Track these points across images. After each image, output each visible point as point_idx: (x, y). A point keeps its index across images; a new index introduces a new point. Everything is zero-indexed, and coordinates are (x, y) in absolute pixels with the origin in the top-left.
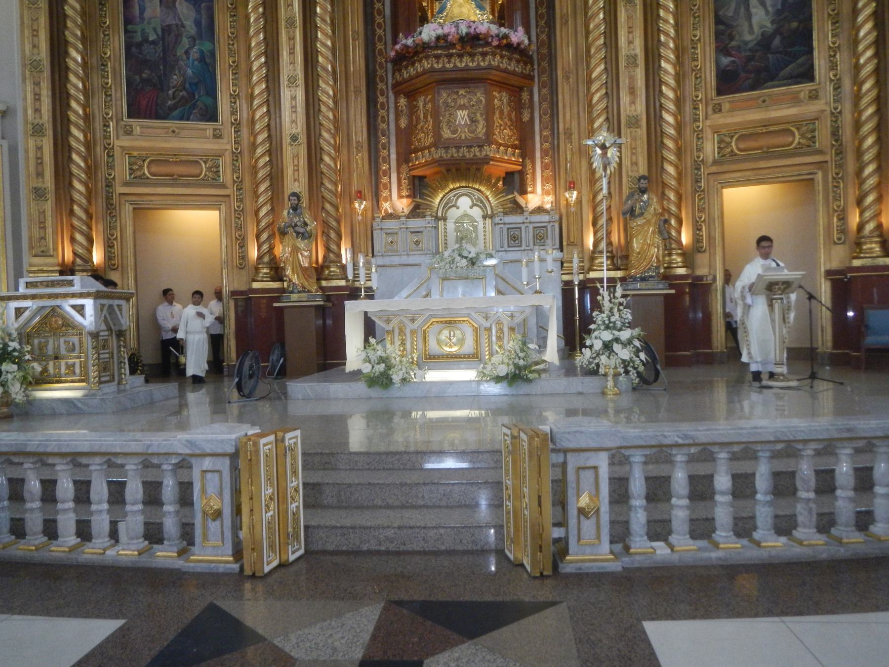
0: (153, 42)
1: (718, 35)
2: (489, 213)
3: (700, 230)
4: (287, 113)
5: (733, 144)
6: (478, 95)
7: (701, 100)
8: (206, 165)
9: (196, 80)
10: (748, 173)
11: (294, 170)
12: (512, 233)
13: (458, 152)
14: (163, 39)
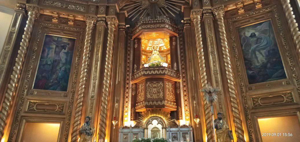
0: (49, 65)
1: (246, 64)
2: (165, 126)
3: (252, 136)
4: (91, 88)
5: (259, 101)
6: (161, 83)
8: (58, 106)
9: (61, 77)
10: (267, 113)
11: (91, 109)
12: (174, 135)
13: (153, 103)
14: (53, 64)
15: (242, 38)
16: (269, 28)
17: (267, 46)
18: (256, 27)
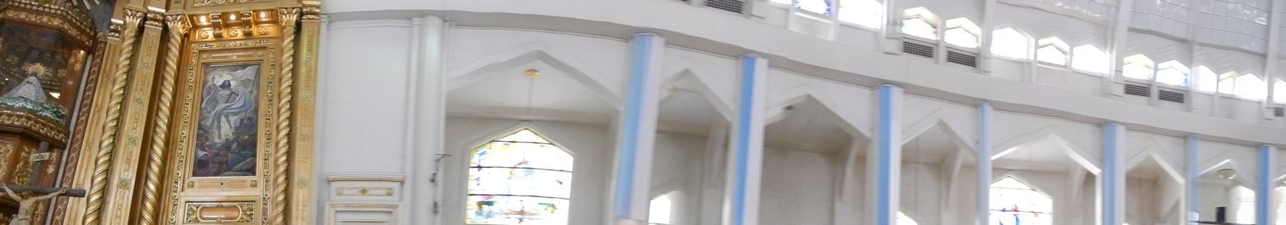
7: (180, 177)
15: (207, 86)
16: (255, 78)
17: (242, 109)
18: (236, 70)
